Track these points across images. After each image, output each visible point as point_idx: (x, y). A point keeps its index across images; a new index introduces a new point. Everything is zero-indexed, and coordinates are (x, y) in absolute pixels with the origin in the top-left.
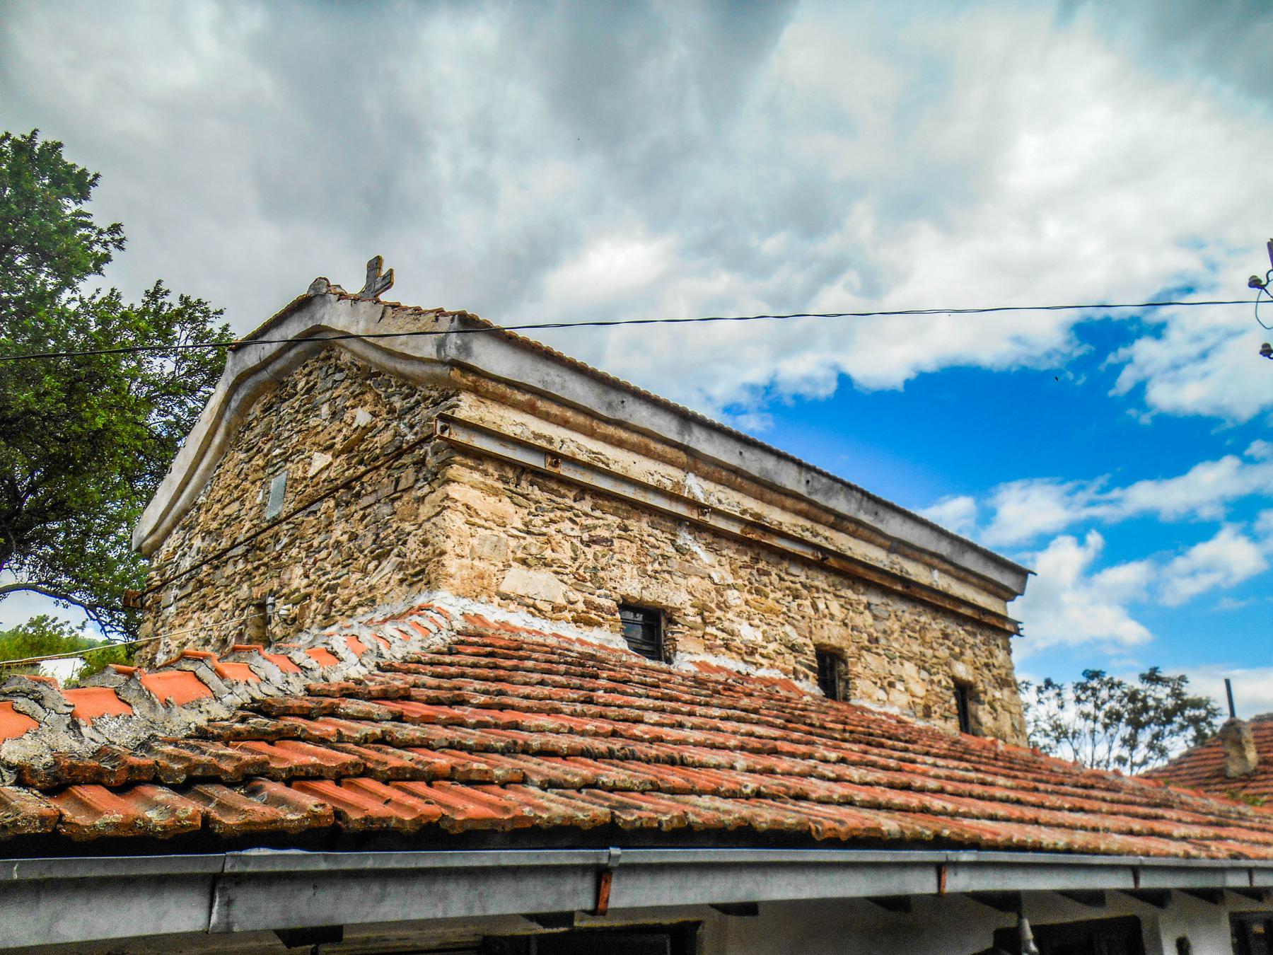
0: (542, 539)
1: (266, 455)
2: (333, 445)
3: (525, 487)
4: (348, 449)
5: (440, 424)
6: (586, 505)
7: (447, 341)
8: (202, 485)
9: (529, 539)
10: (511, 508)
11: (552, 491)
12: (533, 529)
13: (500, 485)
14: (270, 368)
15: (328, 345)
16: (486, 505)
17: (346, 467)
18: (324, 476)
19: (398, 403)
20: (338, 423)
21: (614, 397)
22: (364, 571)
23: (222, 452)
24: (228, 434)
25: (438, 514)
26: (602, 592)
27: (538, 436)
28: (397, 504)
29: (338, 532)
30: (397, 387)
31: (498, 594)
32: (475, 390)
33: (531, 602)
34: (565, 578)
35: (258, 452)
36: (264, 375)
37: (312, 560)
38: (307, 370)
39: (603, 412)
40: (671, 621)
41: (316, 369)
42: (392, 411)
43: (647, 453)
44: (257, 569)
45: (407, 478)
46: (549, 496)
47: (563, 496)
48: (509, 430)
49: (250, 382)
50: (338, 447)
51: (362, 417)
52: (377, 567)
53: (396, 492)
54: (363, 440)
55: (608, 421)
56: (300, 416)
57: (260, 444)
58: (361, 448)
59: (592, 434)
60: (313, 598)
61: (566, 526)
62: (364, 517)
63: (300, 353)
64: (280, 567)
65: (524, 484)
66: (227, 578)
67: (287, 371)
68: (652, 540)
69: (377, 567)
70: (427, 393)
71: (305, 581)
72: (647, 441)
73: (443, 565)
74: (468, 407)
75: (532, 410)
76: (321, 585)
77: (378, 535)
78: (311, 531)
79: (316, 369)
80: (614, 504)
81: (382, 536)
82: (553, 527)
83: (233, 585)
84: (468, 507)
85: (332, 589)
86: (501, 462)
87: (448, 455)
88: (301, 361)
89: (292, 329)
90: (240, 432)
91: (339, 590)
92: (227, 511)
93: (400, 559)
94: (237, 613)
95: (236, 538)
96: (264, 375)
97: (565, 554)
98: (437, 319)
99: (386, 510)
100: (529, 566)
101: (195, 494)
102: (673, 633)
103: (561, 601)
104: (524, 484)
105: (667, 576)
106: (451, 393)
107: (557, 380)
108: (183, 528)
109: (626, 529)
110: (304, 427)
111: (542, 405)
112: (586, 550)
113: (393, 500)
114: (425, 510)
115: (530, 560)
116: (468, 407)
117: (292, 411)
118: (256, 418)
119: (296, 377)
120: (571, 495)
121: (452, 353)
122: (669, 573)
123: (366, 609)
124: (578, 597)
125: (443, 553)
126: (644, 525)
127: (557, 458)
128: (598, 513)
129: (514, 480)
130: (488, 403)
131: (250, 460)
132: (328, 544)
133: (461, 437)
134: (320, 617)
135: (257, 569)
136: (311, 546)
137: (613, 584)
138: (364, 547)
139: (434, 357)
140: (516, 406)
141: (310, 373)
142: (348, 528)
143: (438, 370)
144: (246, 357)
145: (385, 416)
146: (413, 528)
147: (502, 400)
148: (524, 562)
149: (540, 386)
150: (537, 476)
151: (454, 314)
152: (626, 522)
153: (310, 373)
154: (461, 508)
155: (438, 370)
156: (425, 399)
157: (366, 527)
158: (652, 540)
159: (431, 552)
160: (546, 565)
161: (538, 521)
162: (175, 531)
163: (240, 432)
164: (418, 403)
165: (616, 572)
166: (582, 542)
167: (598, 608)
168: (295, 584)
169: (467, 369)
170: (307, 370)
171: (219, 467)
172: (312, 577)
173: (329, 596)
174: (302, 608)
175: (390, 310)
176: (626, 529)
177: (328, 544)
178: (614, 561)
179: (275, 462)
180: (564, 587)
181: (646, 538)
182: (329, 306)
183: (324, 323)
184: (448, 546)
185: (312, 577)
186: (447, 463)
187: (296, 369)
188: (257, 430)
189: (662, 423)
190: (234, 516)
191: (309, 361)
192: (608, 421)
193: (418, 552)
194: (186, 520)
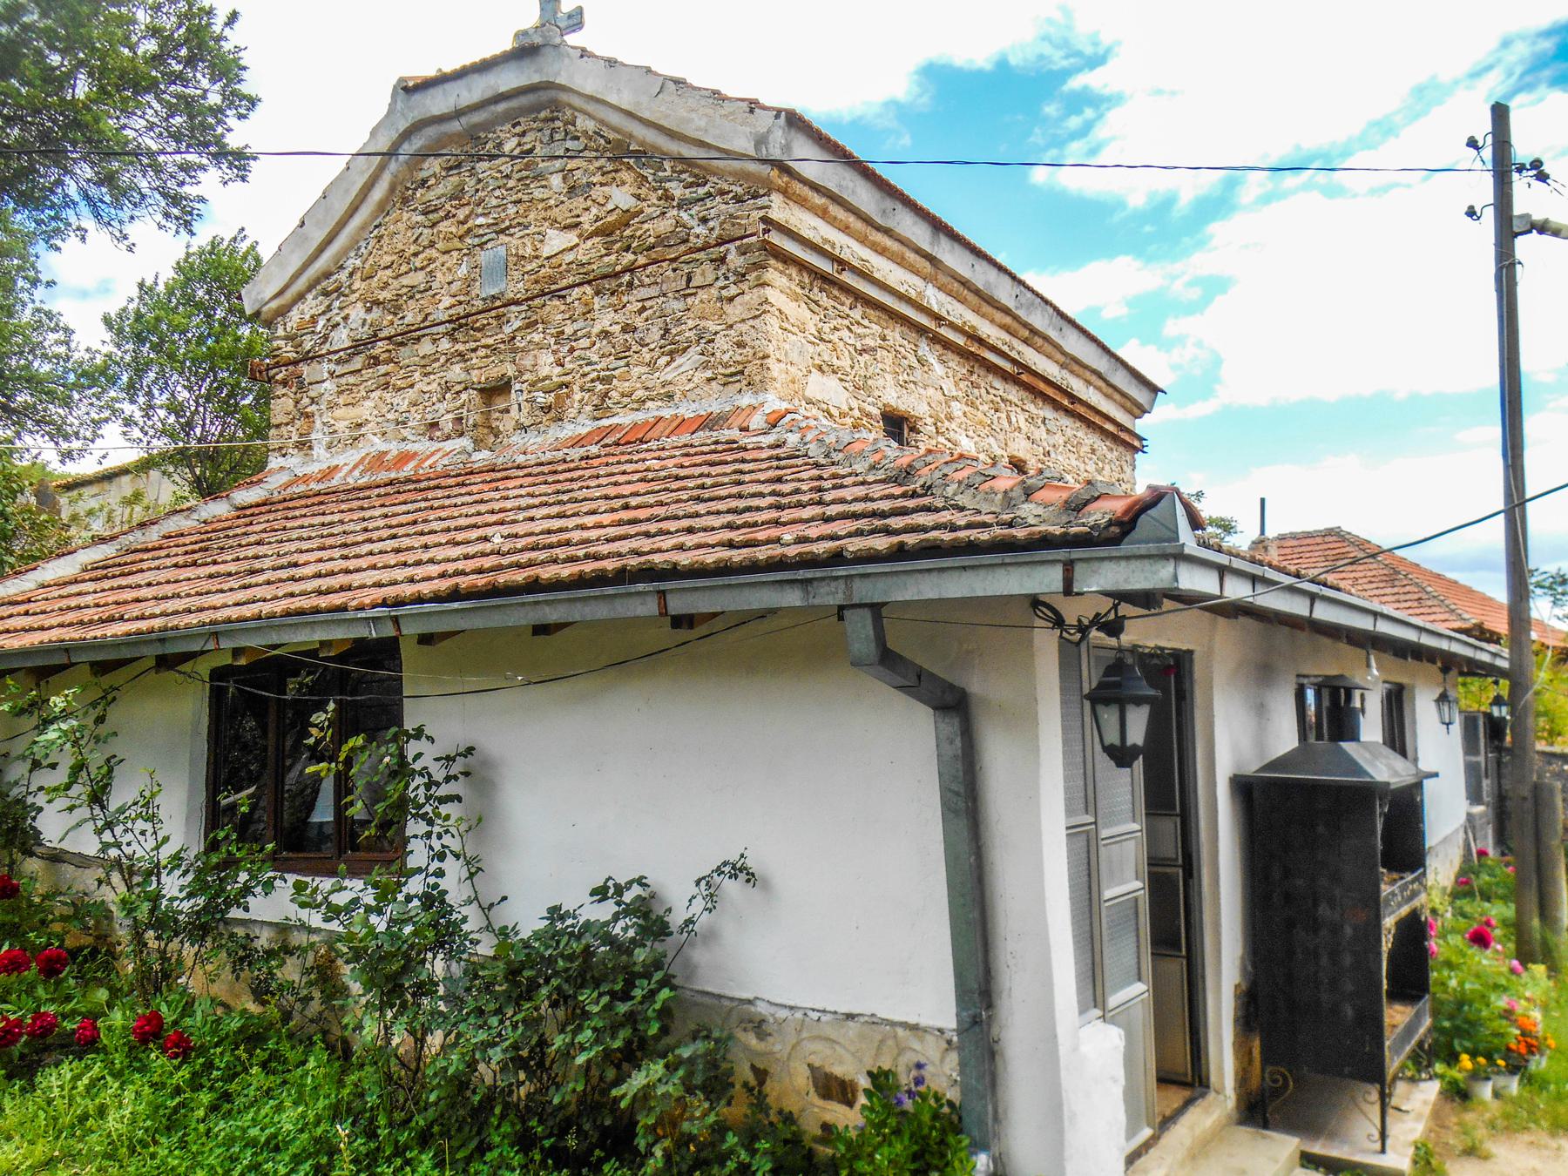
0: (830, 345)
1: (463, 223)
2: (577, 225)
3: (817, 294)
4: (604, 232)
5: (762, 226)
6: (857, 314)
7: (770, 139)
8: (354, 245)
9: (822, 346)
10: (808, 314)
11: (835, 298)
12: (824, 337)
13: (798, 290)
14: (464, 120)
15: (556, 106)
16: (798, 312)
17: (604, 252)
18: (569, 257)
19: (677, 190)
20: (581, 199)
21: (889, 203)
22: (651, 365)
23: (383, 208)
24: (392, 189)
25: (755, 317)
26: (870, 400)
27: (826, 241)
28: (690, 300)
29: (605, 320)
30: (673, 172)
31: (805, 398)
32: (784, 192)
33: (825, 407)
34: (847, 385)
35: (447, 217)
36: (455, 126)
37: (567, 348)
38: (518, 129)
39: (879, 220)
40: (913, 429)
41: (532, 129)
42: (667, 197)
43: (900, 261)
44: (474, 350)
45: (703, 274)
46: (833, 303)
47: (843, 304)
48: (807, 233)
49: (431, 131)
50: (588, 227)
51: (622, 198)
52: (668, 364)
53: (688, 287)
54: (627, 225)
55: (879, 228)
56: (511, 183)
57: (448, 207)
58: (625, 234)
59: (863, 241)
60: (576, 388)
61: (845, 334)
62: (644, 309)
63: (514, 109)
64: (515, 351)
65: (816, 290)
66: (423, 357)
67: (488, 126)
68: (902, 349)
69: (668, 364)
70: (726, 187)
71: (558, 370)
72: (905, 249)
73: (768, 368)
74: (779, 209)
75: (823, 214)
76: (584, 375)
77: (667, 331)
78: (560, 317)
79: (532, 129)
80: (878, 313)
81: (674, 331)
82: (837, 334)
83: (436, 365)
84: (780, 311)
85: (606, 380)
86: (802, 266)
87: (762, 258)
88: (512, 118)
89: (508, 79)
90: (408, 189)
91: (615, 381)
92: (405, 281)
93: (705, 358)
94: (448, 396)
95: (427, 315)
96: (455, 126)
97: (845, 363)
98: (752, 111)
99: (678, 305)
100: (823, 372)
101: (344, 253)
102: (916, 441)
103: (845, 408)
104: (816, 290)
105: (912, 385)
106: (762, 192)
107: (851, 185)
108: (326, 294)
109: (884, 339)
110: (525, 198)
111: (835, 210)
112: (859, 358)
113: (685, 296)
114: (734, 311)
115: (825, 368)
116: (779, 209)
117: (499, 175)
118: (434, 175)
119: (502, 135)
120: (848, 302)
121: (776, 153)
122: (915, 383)
123: (660, 403)
124: (855, 404)
125: (766, 357)
126: (897, 336)
127: (843, 264)
128: (866, 322)
129: (808, 286)
130: (791, 203)
131: (434, 225)
132: (589, 332)
133: (776, 238)
134: (589, 408)
135: (474, 350)
136: (563, 332)
137: (877, 393)
138: (648, 341)
139: (752, 152)
140: (813, 210)
141: (523, 134)
142: (619, 317)
143: (752, 167)
144: (428, 102)
145: (655, 201)
146: (719, 328)
147: (802, 203)
148: (820, 368)
149: (836, 190)
150: (825, 279)
151: (779, 112)
152: (886, 332)
153: (523, 134)
154: (777, 313)
155: (752, 167)
156: (722, 193)
157: (647, 320)
158: (902, 349)
159: (751, 354)
160: (834, 372)
161: (826, 328)
162: (310, 296)
163: (408, 189)
164: (709, 195)
165: (881, 382)
166: (856, 350)
167: (868, 415)
168: (544, 372)
169: (784, 169)
170: (518, 129)
171: (376, 227)
172: (569, 366)
173: (599, 387)
174: (558, 397)
175: (672, 86)
176: (884, 339)
177: (589, 332)
178: (878, 371)
179: (481, 232)
180: (847, 394)
181: (898, 348)
182: (567, 61)
183: (560, 80)
184: (770, 350)
185: (569, 366)
186: (760, 266)
187: (503, 125)
188: (440, 190)
189: (919, 232)
190: (422, 288)
191: (522, 120)
192: (879, 228)
193: (731, 353)
194: (329, 284)
